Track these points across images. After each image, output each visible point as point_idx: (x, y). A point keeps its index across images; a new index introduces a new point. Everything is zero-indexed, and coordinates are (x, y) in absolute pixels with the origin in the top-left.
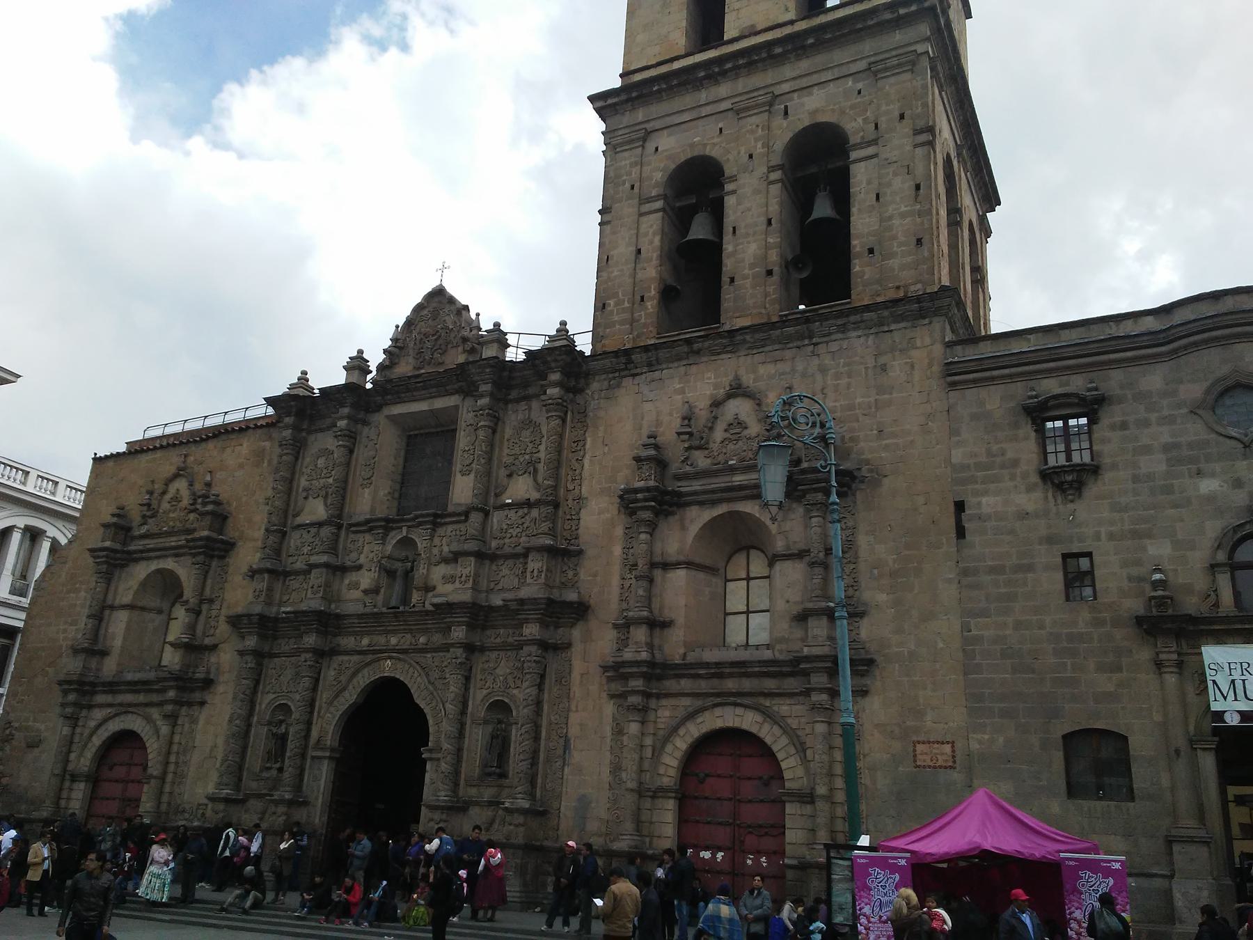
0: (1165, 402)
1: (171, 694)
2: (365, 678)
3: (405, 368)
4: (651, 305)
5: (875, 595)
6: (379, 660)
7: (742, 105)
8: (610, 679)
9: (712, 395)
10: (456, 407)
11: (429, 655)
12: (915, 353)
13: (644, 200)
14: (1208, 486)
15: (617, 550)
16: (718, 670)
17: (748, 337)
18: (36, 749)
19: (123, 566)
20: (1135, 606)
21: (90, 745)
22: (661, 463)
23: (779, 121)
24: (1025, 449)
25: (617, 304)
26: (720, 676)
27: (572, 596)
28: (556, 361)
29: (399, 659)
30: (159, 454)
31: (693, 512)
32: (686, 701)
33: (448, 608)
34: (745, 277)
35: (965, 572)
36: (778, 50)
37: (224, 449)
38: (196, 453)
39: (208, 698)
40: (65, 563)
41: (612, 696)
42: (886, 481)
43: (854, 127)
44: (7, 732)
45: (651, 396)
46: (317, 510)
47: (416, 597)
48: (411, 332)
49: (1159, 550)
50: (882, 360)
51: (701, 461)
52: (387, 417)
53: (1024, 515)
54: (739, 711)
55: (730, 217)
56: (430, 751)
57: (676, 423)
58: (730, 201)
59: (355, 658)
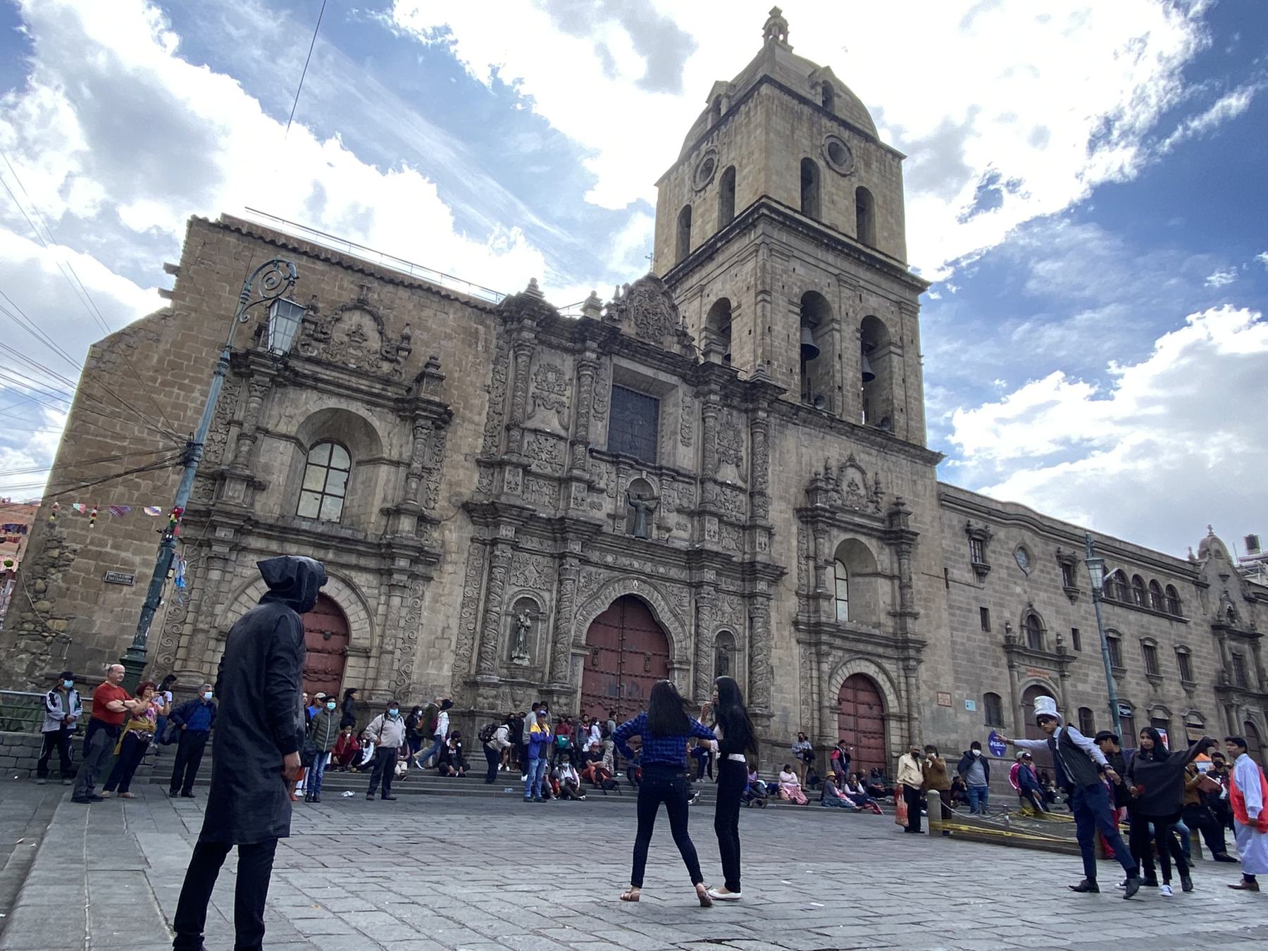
0: (1006, 547)
2: (617, 591)
3: (628, 329)
6: (628, 578)
7: (845, 279)
8: (798, 630)
9: (838, 461)
10: (675, 386)
11: (668, 584)
12: (927, 480)
14: (1018, 590)
15: (794, 543)
17: (860, 433)
18: (125, 589)
19: (280, 385)
21: (243, 598)
24: (966, 549)
25: (779, 366)
26: (858, 641)
28: (772, 395)
29: (645, 582)
30: (320, 266)
31: (835, 532)
32: (840, 653)
34: (848, 391)
35: (950, 607)
36: (863, 259)
37: (421, 307)
38: (378, 294)
39: (435, 574)
40: (158, 341)
41: (798, 642)
44: (56, 553)
45: (806, 444)
48: (632, 300)
49: (1007, 614)
50: (915, 478)
52: (615, 365)
54: (868, 663)
56: (680, 663)
59: (605, 574)
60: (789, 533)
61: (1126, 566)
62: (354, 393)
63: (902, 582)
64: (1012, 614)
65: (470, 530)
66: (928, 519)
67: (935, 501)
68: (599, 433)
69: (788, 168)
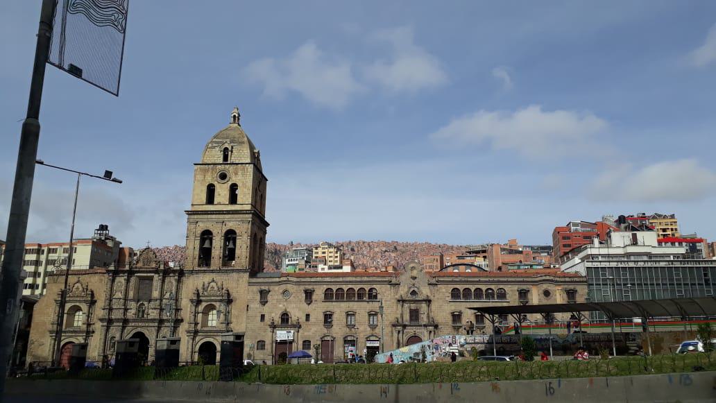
1: (84, 334)
2: (134, 332)
4: (197, 260)
5: (233, 320)
12: (244, 279)
13: (196, 237)
14: (281, 306)
16: (207, 332)
20: (269, 323)
22: (198, 294)
23: (224, 226)
24: (258, 297)
27: (179, 318)
33: (155, 319)
35: (247, 317)
38: (82, 277)
42: (237, 302)
43: (237, 231)
46: (119, 295)
47: (145, 316)
49: (273, 315)
51: (206, 293)
53: (256, 308)
55: (214, 244)
57: (201, 286)
58: (214, 241)
60: (187, 307)
61: (344, 286)
62: (77, 301)
63: (227, 314)
64: (276, 314)
65: (101, 324)
66: (242, 291)
67: (247, 284)
68: (131, 294)
69: (202, 191)
